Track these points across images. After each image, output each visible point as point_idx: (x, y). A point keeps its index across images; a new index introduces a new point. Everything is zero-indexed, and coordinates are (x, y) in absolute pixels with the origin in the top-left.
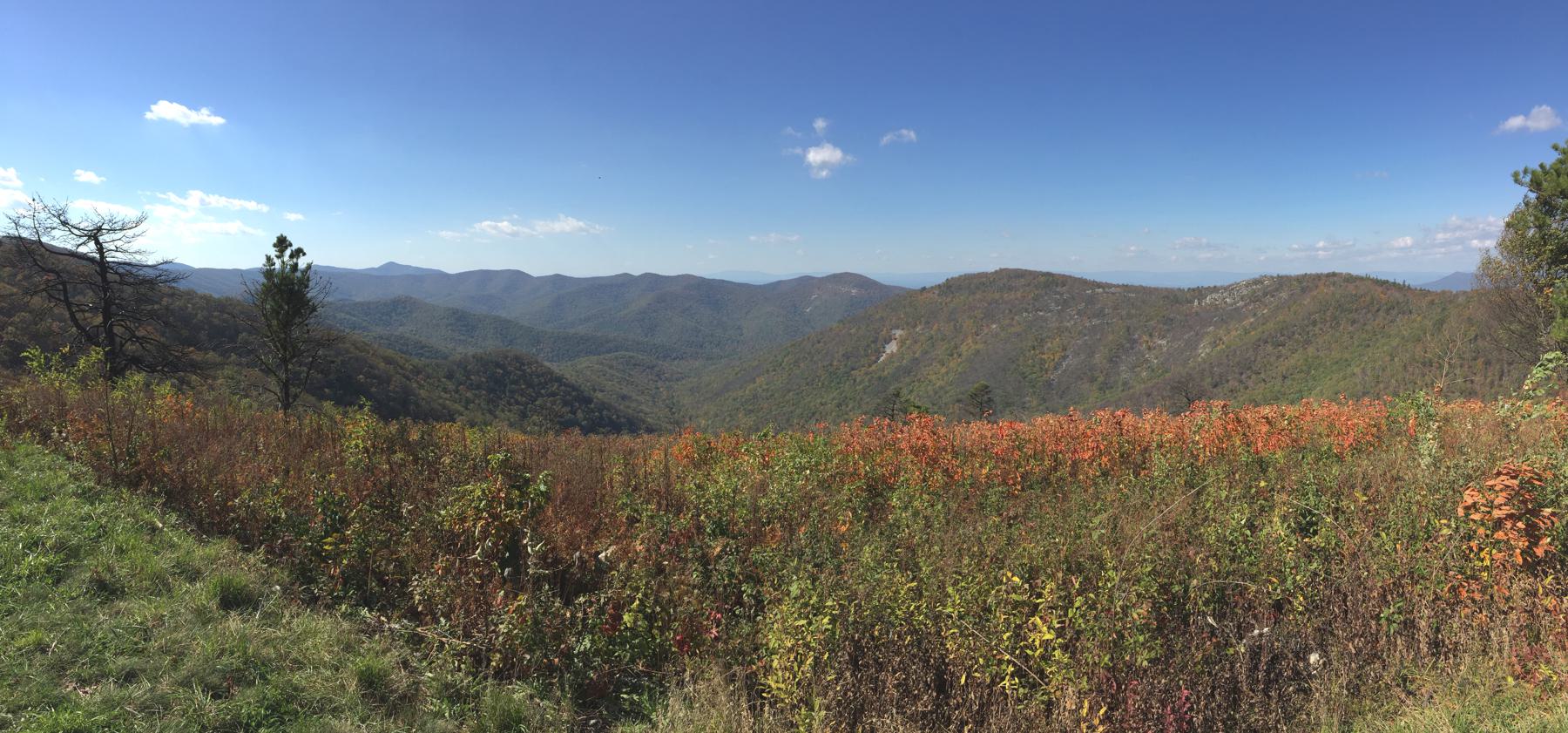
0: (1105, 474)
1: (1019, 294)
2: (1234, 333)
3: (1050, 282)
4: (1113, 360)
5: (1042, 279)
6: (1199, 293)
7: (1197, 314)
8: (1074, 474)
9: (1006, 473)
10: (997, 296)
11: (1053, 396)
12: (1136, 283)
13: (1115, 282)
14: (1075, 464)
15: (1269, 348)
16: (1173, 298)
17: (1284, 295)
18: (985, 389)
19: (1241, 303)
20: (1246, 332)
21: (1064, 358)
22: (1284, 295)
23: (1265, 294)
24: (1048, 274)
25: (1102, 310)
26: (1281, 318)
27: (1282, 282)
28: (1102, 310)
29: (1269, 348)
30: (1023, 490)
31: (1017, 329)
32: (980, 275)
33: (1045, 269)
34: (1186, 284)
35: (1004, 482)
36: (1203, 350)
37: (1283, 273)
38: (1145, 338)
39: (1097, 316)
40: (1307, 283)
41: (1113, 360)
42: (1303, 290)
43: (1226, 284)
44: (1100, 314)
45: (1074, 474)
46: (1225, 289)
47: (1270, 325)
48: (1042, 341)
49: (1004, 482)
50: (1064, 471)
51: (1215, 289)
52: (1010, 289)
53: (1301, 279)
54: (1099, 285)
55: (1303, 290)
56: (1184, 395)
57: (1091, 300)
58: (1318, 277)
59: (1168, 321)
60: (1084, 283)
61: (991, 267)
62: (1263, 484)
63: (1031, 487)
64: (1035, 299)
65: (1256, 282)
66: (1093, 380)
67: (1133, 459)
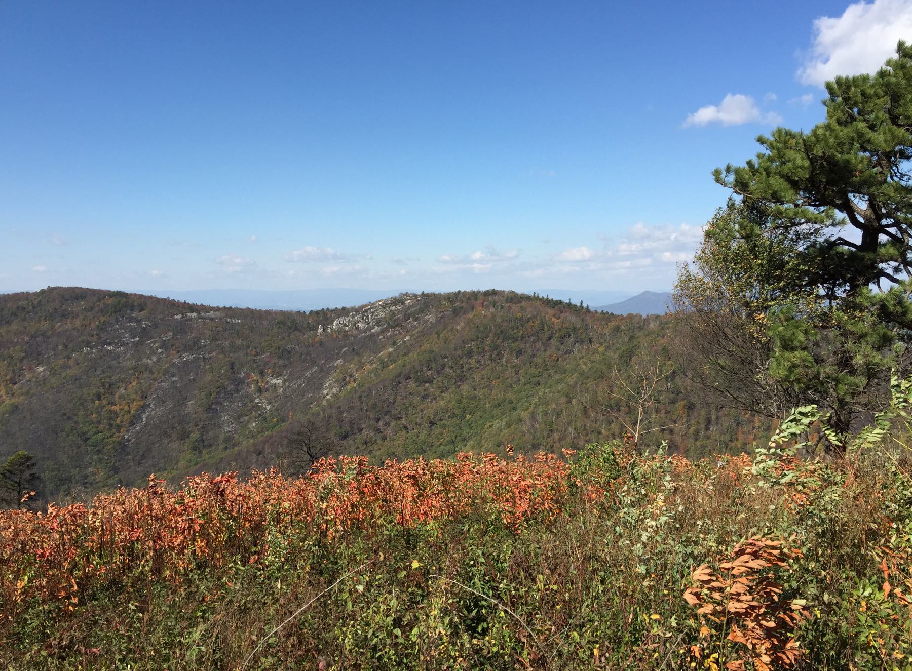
0: (200, 566)
1: (78, 323)
2: (368, 367)
3: (122, 305)
4: (212, 408)
5: (110, 301)
6: (324, 316)
7: (321, 344)
8: (157, 570)
9: (54, 584)
10: (45, 325)
11: (126, 463)
12: (243, 306)
13: (214, 304)
14: (159, 555)
15: (412, 385)
16: (291, 324)
17: (431, 318)
18: (27, 462)
19: (377, 329)
20: (384, 365)
21: (144, 408)
22: (431, 318)
23: (407, 317)
24: (119, 294)
25: (196, 342)
26: (426, 346)
27: (428, 301)
28: (196, 342)
29: (412, 385)
30: (82, 603)
31: (71, 372)
32: (17, 297)
33: (114, 288)
34: (307, 306)
35: (53, 597)
36: (329, 390)
37: (428, 290)
38: (254, 377)
39: (189, 348)
40: (460, 303)
41: (212, 408)
42: (456, 312)
43: (357, 304)
44: (194, 346)
45: (157, 570)
46: (357, 310)
47: (414, 356)
48: (111, 388)
49: (53, 597)
50: (145, 566)
51: (344, 312)
52: (65, 316)
53: (454, 298)
54: (192, 308)
55: (456, 312)
56: (305, 450)
57: (182, 328)
58: (474, 295)
60: (170, 305)
61: (35, 286)
62: (415, 564)
63: (93, 597)
64: (102, 328)
65: (396, 301)
66: (184, 436)
67: (241, 539)
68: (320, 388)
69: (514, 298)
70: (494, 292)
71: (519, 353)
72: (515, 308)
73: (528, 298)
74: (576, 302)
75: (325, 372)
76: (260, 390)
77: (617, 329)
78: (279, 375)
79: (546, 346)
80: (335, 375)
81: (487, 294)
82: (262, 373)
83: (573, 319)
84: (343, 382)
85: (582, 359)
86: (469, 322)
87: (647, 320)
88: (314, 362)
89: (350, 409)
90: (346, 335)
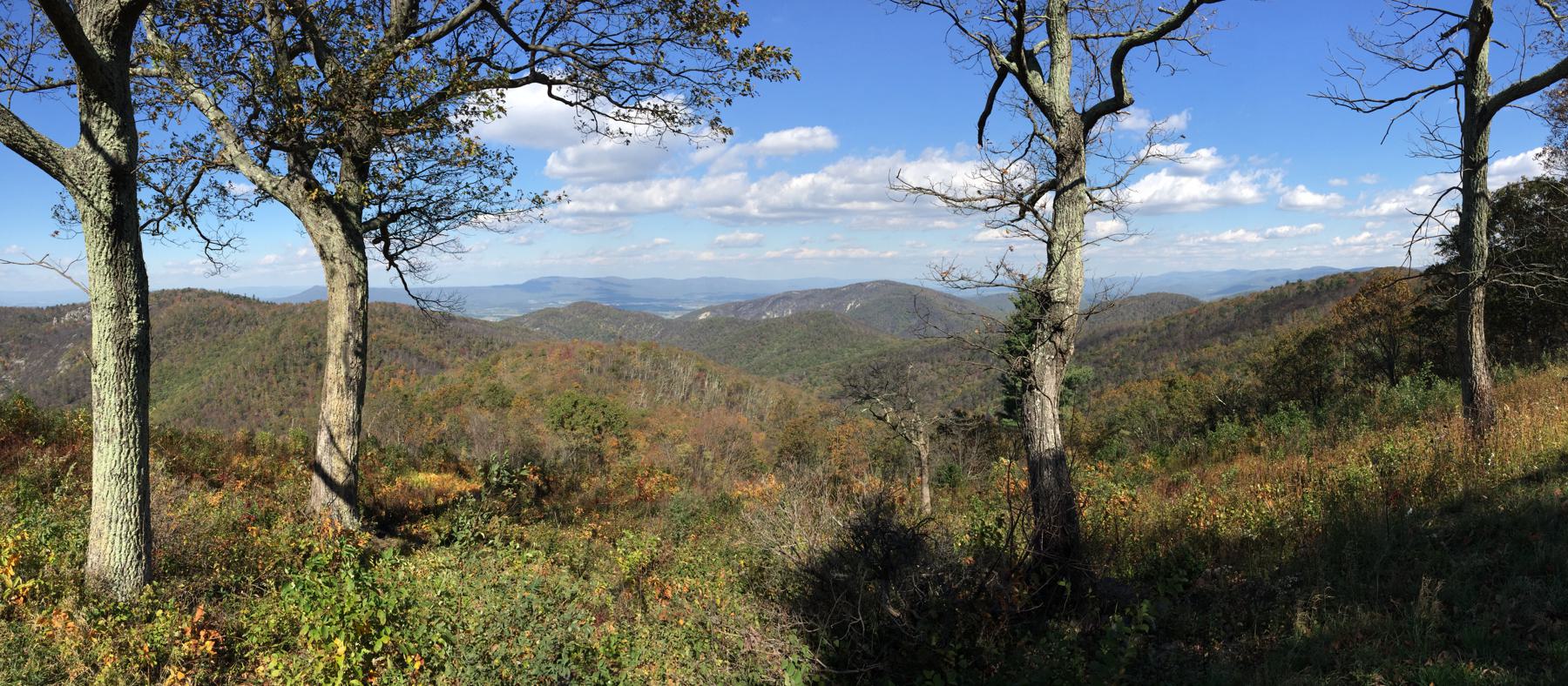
6: (58, 311)
7: (56, 332)
34: (43, 303)
51: (75, 307)
58: (175, 292)
59: (26, 340)
68: (55, 365)
69: (204, 294)
70: (190, 290)
71: (206, 334)
72: (204, 301)
73: (214, 294)
74: (250, 295)
75: (59, 353)
76: (6, 369)
77: (274, 314)
78: (22, 357)
79: (225, 329)
80: (66, 355)
81: (184, 291)
82: (7, 356)
83: (246, 308)
84: (73, 360)
85: (250, 336)
86: (170, 312)
87: (295, 308)
88: (50, 346)
89: (76, 380)
90: (76, 325)
